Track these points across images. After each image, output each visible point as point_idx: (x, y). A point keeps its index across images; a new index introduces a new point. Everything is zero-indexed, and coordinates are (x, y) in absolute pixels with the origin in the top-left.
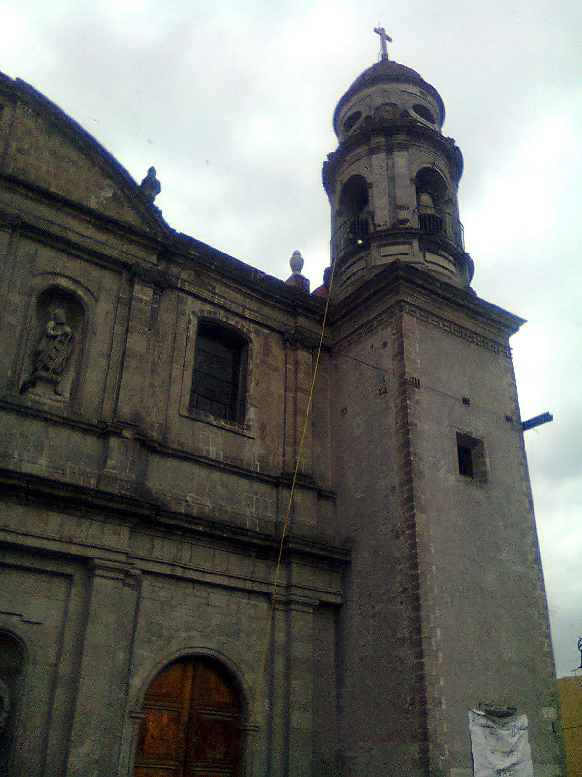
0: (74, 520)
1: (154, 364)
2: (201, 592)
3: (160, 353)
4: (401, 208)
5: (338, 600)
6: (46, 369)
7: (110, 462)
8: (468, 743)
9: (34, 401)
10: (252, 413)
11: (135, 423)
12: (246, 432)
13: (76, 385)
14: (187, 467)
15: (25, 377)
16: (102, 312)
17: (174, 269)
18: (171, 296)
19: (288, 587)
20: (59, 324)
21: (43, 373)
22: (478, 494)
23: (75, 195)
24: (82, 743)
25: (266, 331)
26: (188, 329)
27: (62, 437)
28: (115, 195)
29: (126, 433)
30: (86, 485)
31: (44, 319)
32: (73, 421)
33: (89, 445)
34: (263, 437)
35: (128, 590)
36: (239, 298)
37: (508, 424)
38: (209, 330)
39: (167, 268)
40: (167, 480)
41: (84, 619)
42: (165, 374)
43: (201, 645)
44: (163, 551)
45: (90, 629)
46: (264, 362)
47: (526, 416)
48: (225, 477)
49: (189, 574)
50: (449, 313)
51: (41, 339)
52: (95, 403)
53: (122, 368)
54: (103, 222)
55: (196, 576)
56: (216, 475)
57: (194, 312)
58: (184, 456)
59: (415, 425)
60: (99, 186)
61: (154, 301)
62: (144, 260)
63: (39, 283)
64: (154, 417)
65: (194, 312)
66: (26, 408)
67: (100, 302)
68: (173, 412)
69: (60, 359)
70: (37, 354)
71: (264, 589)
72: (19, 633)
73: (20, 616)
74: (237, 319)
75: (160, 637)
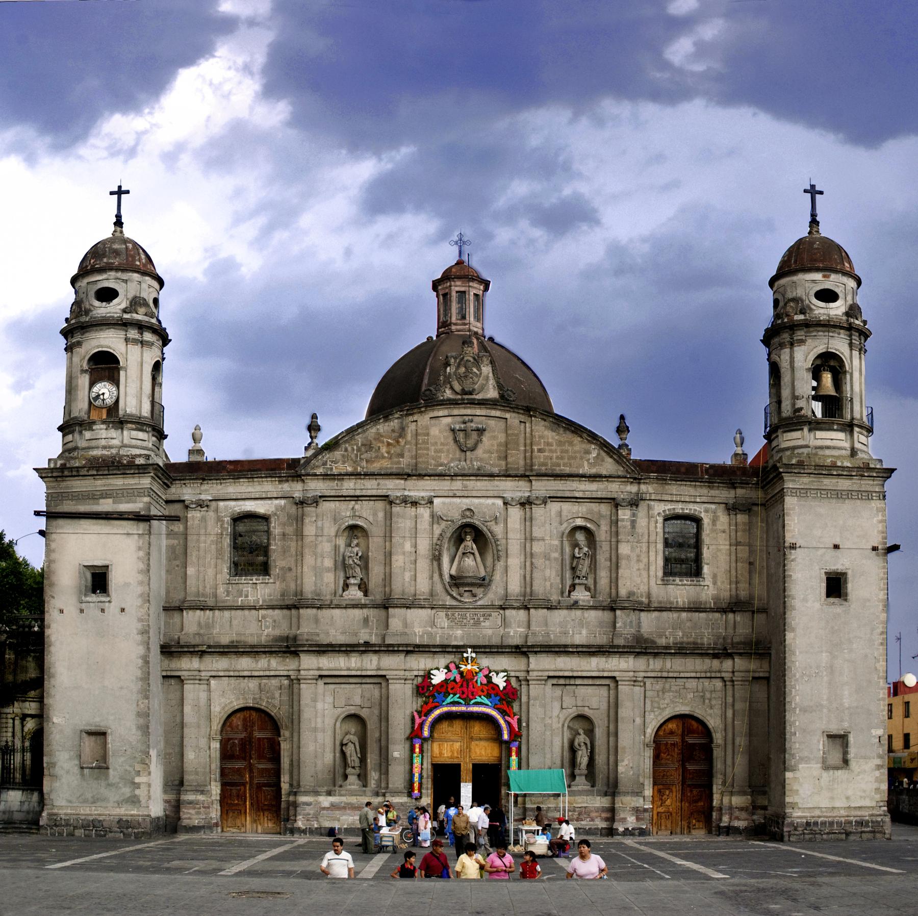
0: (604, 659)
5: (767, 675)
10: (706, 569)
12: (702, 583)
15: (569, 583)
18: (643, 505)
19: (733, 672)
21: (577, 581)
24: (623, 761)
26: (656, 527)
35: (637, 688)
42: (645, 560)
46: (713, 531)
48: (690, 614)
49: (671, 675)
53: (617, 567)
55: (675, 675)
56: (684, 615)
59: (791, 576)
60: (588, 452)
61: (634, 515)
63: (566, 527)
71: (718, 675)
75: (659, 708)
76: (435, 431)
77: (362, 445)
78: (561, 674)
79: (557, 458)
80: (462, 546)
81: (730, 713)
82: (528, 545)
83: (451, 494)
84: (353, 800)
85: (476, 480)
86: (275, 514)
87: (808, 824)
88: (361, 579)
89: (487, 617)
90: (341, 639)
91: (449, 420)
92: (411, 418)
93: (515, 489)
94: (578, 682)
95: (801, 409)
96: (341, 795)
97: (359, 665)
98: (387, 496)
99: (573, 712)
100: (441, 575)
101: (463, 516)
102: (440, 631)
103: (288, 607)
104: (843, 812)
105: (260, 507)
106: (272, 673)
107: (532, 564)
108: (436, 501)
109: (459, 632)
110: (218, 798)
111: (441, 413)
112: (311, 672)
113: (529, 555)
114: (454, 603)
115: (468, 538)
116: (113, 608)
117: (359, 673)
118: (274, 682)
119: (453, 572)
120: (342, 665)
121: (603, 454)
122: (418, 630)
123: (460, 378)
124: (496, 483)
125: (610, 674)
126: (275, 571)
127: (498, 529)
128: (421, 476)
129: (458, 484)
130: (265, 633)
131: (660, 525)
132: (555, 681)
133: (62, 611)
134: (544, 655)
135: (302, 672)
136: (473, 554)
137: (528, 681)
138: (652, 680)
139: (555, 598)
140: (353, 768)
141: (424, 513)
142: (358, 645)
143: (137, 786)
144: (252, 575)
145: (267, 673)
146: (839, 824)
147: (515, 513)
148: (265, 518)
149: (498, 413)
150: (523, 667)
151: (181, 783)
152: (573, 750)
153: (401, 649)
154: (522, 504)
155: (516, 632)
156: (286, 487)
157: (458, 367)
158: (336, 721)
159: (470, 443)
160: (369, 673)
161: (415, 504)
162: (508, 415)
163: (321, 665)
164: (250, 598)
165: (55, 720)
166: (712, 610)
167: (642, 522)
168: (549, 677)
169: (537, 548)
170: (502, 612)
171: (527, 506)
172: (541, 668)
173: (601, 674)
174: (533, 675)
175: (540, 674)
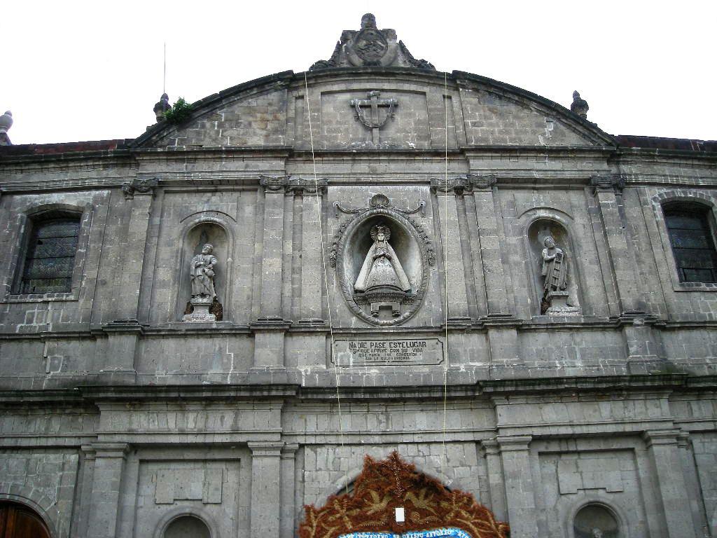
0: (621, 404)
1: (637, 256)
3: (639, 244)
6: (555, 289)
7: (632, 349)
9: (554, 317)
11: (641, 310)
13: (582, 293)
14: (696, 334)
16: (579, 226)
17: (625, 168)
18: (630, 191)
21: (552, 293)
23: (526, 141)
27: (587, 340)
29: (636, 321)
30: (619, 374)
31: (537, 248)
32: (592, 324)
33: (610, 339)
35: (683, 450)
36: (689, 171)
38: (672, 209)
39: (619, 169)
41: (656, 481)
42: (649, 261)
45: (663, 488)
51: (541, 266)
52: (602, 304)
53: (613, 268)
57: (654, 199)
60: (542, 126)
61: (619, 202)
62: (598, 171)
63: (525, 222)
64: (654, 300)
65: (654, 199)
66: (552, 324)
67: (576, 219)
68: (668, 290)
69: (561, 277)
70: (543, 278)
72: (608, 502)
73: (605, 489)
74: (694, 190)
77: (226, 120)
78: (553, 431)
79: (500, 132)
82: (474, 243)
83: (353, 180)
85: (389, 161)
86: (93, 208)
88: (215, 300)
89: (418, 348)
91: (347, 96)
92: (295, 93)
94: (582, 446)
97: (201, 425)
99: (580, 500)
100: (341, 285)
101: (374, 207)
102: (341, 370)
105: (71, 200)
106: (51, 442)
107: (483, 265)
109: (374, 371)
111: (336, 88)
112: (117, 438)
113: (474, 256)
114: (362, 325)
115: (381, 237)
117: (200, 439)
118: (54, 458)
119: (360, 284)
120: (172, 425)
121: (562, 127)
124: (417, 165)
127: (426, 223)
128: (307, 156)
129: (362, 167)
130: (49, 377)
132: (542, 448)
134: (521, 400)
135: (101, 438)
136: (390, 259)
137: (498, 446)
138: (700, 436)
139: (524, 316)
141: (315, 203)
145: (43, 442)
147: (448, 202)
148: (72, 217)
149: (413, 87)
153: (274, 393)
154: (459, 191)
155: (469, 368)
156: (113, 173)
158: (157, 526)
160: (218, 439)
161: (299, 191)
162: (426, 89)
163: (135, 426)
164: (34, 324)
170: (441, 338)
171: (465, 192)
172: (519, 422)
173: (620, 429)
174: (505, 435)
175: (519, 432)
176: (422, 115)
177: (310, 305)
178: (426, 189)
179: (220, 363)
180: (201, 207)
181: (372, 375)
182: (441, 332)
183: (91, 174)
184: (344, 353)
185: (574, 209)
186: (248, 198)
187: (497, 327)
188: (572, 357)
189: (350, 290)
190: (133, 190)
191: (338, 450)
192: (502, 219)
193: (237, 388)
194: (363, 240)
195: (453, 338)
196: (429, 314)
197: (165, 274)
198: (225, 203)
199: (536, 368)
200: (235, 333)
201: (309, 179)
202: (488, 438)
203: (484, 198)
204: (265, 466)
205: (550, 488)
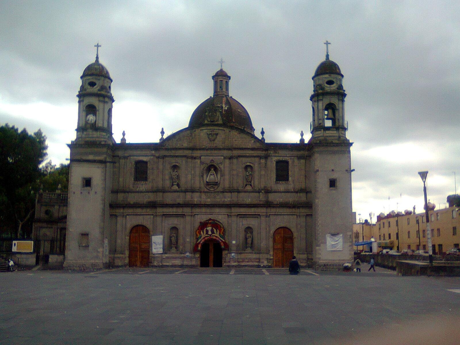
2: (282, 216)
4: (320, 119)
8: (325, 240)
10: (290, 179)
12: (289, 183)
15: (245, 184)
16: (256, 167)
17: (269, 152)
20: (249, 173)
22: (334, 192)
23: (246, 147)
25: (293, 157)
27: (252, 194)
28: (254, 141)
34: (293, 183)
37: (346, 172)
38: (278, 162)
40: (272, 197)
43: (282, 225)
44: (273, 210)
47: (352, 169)
50: (330, 149)
54: (253, 149)
56: (283, 194)
58: (275, 192)
63: (244, 165)
70: (246, 179)
76: (202, 134)
78: (241, 213)
80: (210, 172)
81: (299, 226)
84: (174, 255)
87: (325, 265)
88: (178, 183)
90: (171, 202)
91: (206, 131)
92: (194, 130)
93: (226, 153)
95: (320, 124)
96: (169, 254)
98: (186, 156)
101: (211, 162)
103: (153, 192)
104: (337, 262)
105: (145, 159)
106: (147, 214)
108: (202, 157)
110: (128, 255)
114: (208, 191)
115: (212, 169)
116: (92, 193)
118: (148, 217)
119: (207, 180)
122: (196, 200)
123: (210, 117)
125: (258, 214)
126: (150, 180)
127: (222, 166)
128: (197, 149)
129: (209, 152)
131: (275, 164)
132: (240, 216)
133: (74, 193)
140: (174, 245)
141: (198, 161)
142: (176, 204)
143: (98, 252)
144: (142, 181)
146: (336, 265)
147: (227, 161)
148: (146, 163)
150: (230, 211)
151: (115, 251)
152: (246, 239)
157: (209, 112)
159: (213, 138)
160: (180, 213)
161: (195, 158)
162: (225, 129)
165: (70, 230)
166: (292, 192)
167: (269, 163)
168: (238, 215)
169: (235, 173)
172: (236, 211)
176: (223, 136)
177: (197, 185)
178: (223, 157)
179: (180, 198)
180: (173, 161)
181: (209, 201)
182: (223, 192)
183: (148, 152)
184: (203, 196)
185: (256, 164)
186: (184, 159)
187: (233, 192)
188: (247, 198)
189: (205, 182)
190: (158, 157)
191: (202, 215)
192: (239, 165)
193: (183, 204)
194: (209, 169)
195: (225, 193)
196: (220, 189)
197: (167, 177)
198: (179, 160)
199: (240, 201)
200: (182, 192)
201: (197, 155)
202: (229, 214)
203: (235, 161)
204: (188, 218)
205: (241, 224)
